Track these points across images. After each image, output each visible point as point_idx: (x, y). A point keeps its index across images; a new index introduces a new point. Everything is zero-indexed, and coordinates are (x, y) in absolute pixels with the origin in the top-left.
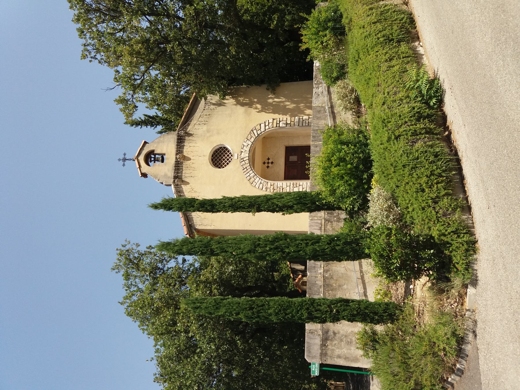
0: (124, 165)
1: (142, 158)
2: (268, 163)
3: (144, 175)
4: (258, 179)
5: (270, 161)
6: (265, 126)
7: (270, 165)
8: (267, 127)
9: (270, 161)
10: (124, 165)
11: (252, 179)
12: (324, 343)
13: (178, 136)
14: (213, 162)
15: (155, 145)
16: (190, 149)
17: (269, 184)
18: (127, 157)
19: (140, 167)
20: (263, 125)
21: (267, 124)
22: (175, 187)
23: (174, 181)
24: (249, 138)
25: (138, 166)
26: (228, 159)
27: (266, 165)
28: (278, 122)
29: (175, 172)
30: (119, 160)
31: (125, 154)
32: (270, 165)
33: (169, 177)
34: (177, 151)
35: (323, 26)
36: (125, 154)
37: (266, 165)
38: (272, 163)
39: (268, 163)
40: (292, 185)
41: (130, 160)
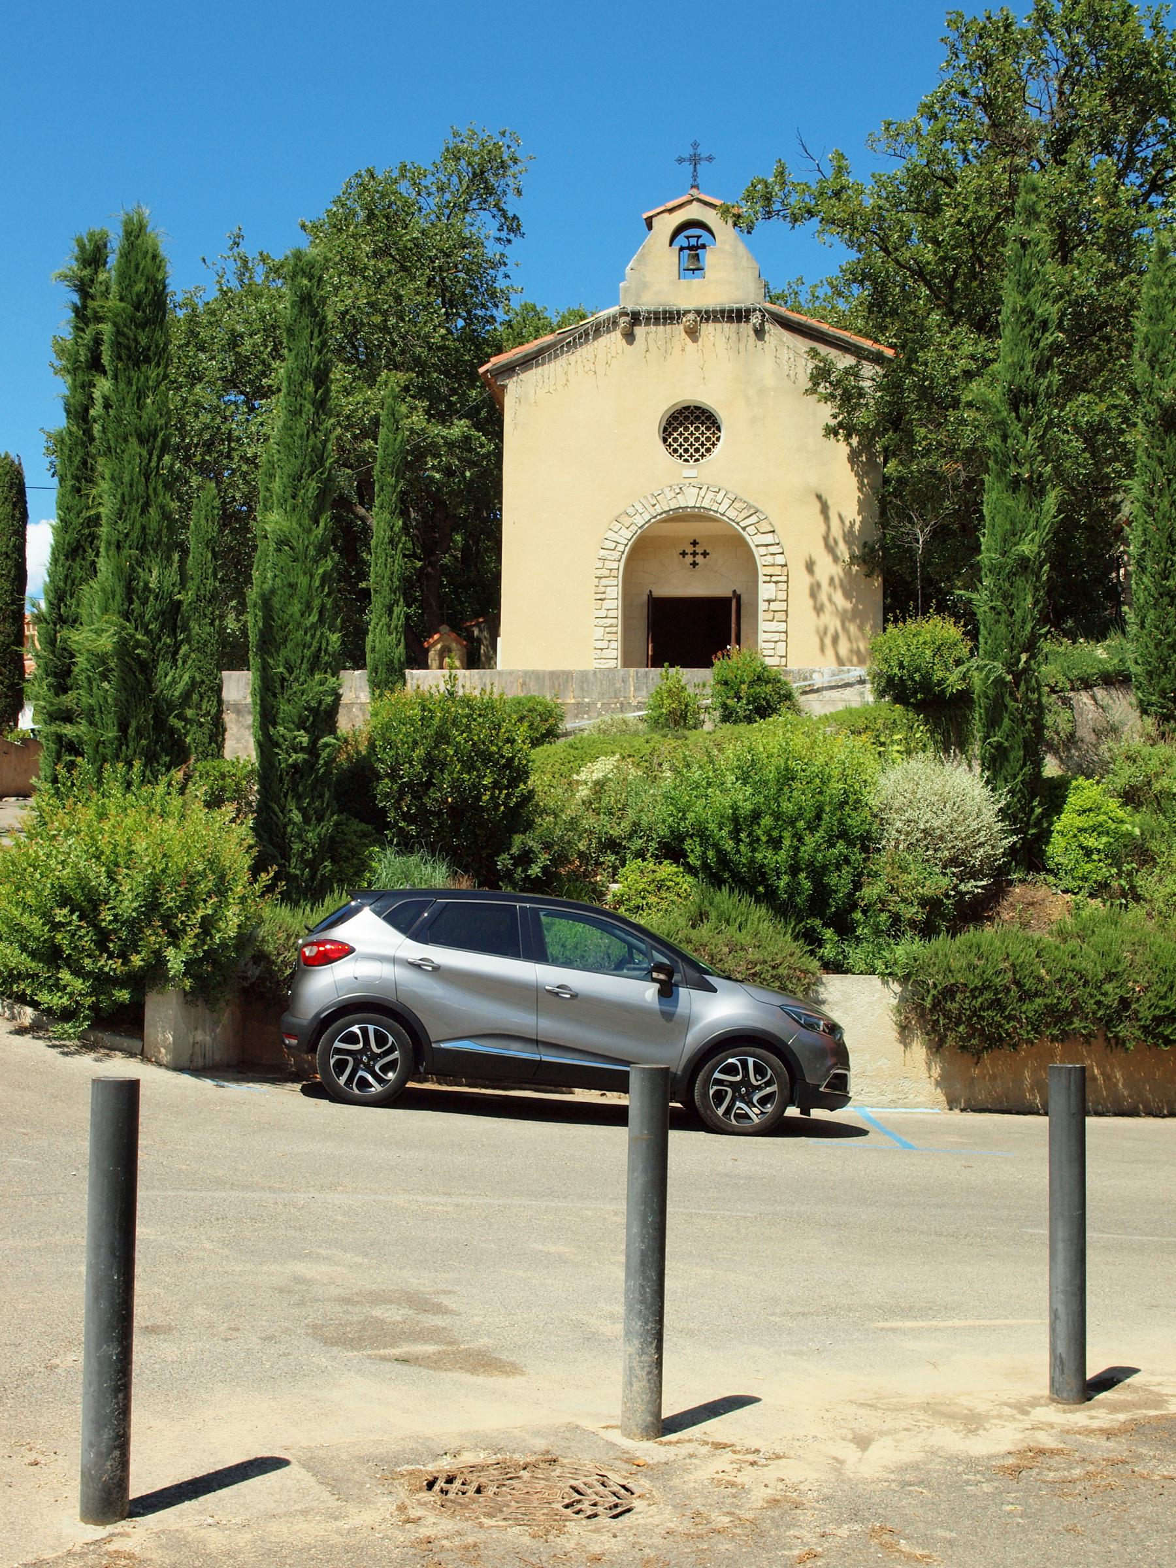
0: (680, 160)
1: (694, 212)
2: (694, 554)
3: (649, 223)
5: (699, 559)
7: (689, 559)
8: (763, 550)
9: (699, 559)
10: (680, 160)
11: (627, 521)
13: (748, 311)
14: (680, 412)
15: (727, 247)
16: (721, 342)
17: (615, 565)
19: (671, 211)
20: (769, 539)
21: (773, 549)
22: (609, 319)
24: (737, 505)
25: (670, 205)
26: (686, 451)
27: (690, 549)
28: (774, 579)
29: (649, 312)
30: (695, 145)
31: (710, 159)
32: (689, 559)
33: (638, 296)
34: (707, 312)
35: (675, 693)
36: (710, 159)
37: (690, 549)
38: (694, 564)
39: (694, 554)
41: (695, 177)
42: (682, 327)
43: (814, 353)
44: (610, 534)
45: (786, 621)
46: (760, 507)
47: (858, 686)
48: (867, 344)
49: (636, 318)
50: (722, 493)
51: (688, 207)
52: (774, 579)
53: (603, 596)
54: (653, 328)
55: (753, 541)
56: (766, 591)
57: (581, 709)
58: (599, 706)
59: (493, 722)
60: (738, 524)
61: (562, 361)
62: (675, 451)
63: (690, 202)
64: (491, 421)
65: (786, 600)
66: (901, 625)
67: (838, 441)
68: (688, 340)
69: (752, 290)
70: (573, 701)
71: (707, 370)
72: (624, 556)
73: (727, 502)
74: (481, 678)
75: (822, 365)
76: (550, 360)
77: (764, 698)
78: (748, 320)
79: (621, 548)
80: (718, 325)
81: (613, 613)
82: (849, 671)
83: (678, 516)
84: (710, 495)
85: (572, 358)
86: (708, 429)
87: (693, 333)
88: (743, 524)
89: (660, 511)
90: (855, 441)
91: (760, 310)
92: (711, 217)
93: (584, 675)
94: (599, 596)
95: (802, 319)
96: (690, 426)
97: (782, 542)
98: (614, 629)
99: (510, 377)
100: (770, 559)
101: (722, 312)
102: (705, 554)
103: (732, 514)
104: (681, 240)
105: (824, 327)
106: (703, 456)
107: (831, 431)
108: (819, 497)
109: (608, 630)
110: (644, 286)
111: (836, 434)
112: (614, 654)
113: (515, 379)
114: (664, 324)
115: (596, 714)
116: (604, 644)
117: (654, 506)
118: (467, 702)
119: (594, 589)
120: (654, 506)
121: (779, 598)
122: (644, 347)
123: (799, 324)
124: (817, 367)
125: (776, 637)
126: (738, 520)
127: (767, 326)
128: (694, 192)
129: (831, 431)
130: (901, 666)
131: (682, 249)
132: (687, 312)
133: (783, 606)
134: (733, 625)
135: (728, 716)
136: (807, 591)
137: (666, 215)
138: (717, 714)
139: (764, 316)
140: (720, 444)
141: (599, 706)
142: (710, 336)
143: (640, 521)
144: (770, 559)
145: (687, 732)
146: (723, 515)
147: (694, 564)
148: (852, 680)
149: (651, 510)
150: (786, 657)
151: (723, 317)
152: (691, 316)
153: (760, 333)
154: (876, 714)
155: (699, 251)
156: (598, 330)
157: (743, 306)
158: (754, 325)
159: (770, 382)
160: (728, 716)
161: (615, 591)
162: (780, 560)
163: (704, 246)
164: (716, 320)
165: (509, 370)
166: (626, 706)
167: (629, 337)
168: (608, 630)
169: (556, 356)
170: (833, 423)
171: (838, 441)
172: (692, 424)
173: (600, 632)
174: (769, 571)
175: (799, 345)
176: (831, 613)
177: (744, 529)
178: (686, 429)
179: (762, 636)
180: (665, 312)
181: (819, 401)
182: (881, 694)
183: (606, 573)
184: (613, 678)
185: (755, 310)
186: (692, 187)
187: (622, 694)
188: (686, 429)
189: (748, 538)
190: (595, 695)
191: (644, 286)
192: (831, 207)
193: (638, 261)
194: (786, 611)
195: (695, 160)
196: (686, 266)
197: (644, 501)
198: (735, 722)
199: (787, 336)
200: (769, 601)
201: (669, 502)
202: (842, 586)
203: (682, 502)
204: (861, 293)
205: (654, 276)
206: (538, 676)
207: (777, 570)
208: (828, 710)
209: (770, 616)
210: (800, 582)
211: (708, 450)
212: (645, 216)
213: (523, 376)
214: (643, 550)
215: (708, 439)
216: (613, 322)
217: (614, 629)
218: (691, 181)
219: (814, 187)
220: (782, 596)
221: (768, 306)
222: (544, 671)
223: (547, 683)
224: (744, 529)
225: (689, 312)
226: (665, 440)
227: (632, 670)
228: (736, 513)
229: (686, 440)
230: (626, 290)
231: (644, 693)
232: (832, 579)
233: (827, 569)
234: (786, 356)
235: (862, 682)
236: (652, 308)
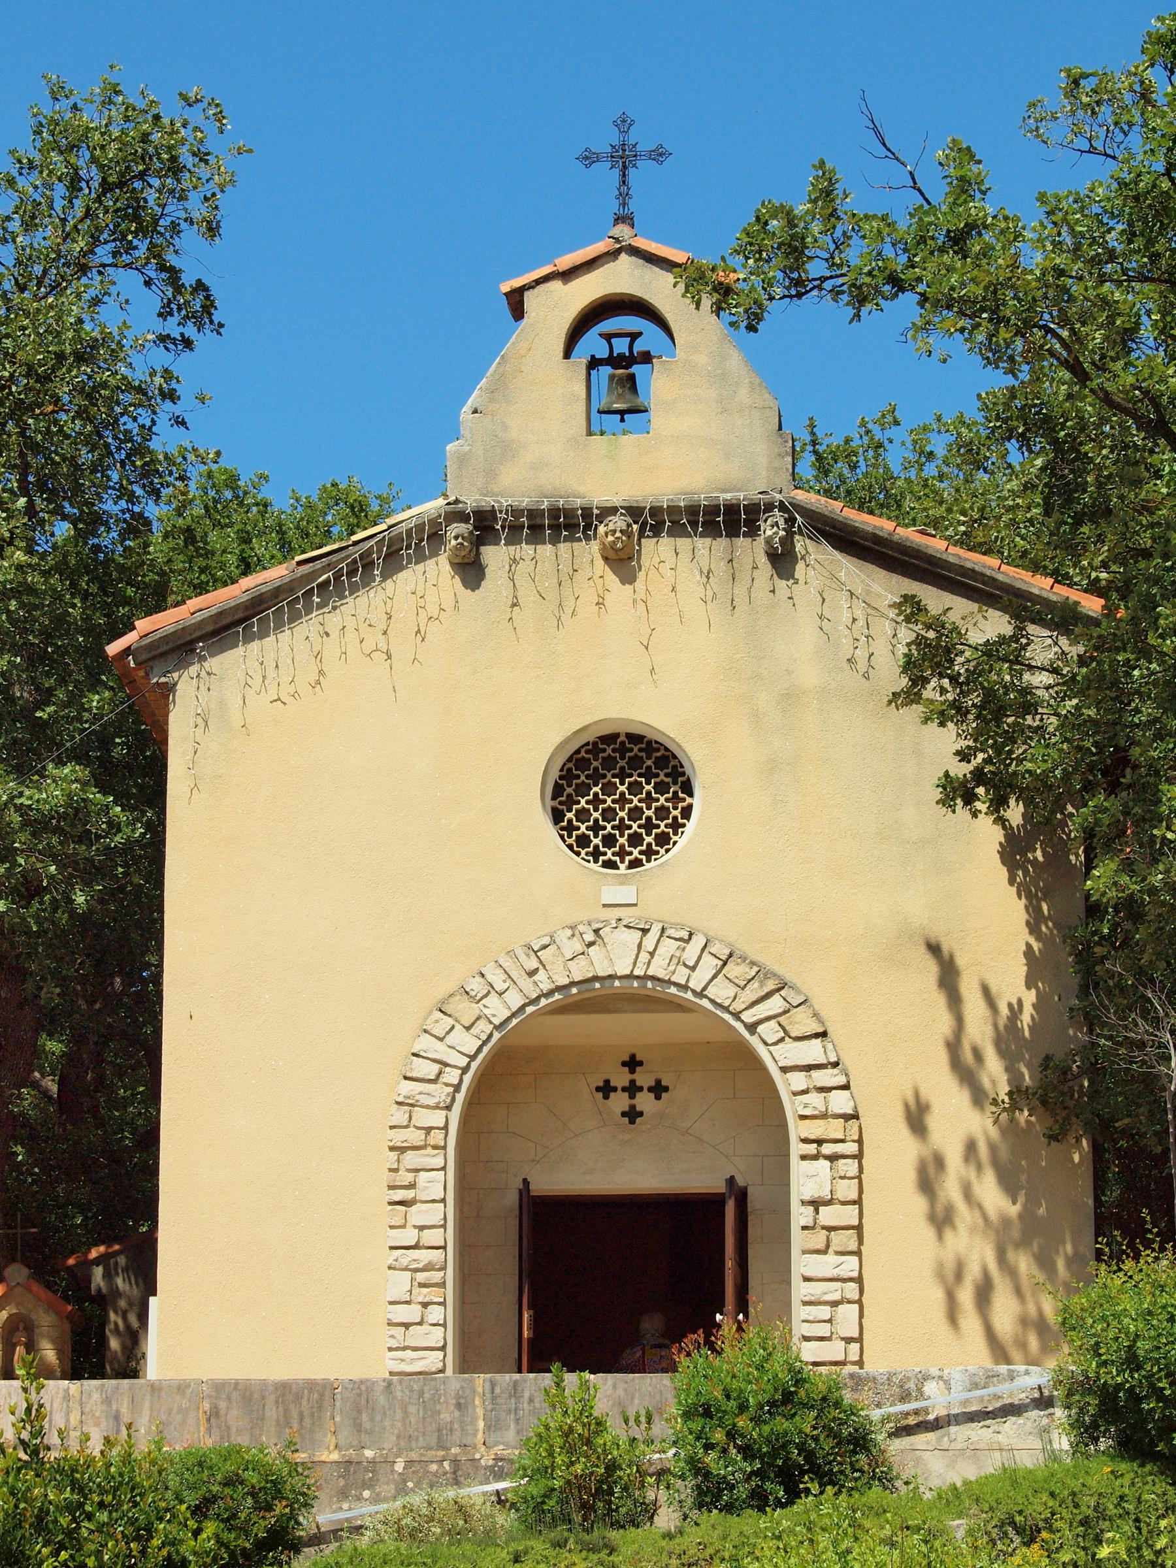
0: (589, 159)
1: (622, 278)
2: (632, 1089)
3: (516, 303)
4: (471, 1046)
5: (645, 1101)
6: (809, 1068)
7: (620, 1102)
8: (798, 1080)
9: (645, 1101)
10: (589, 159)
11: (465, 1010)
17: (437, 1118)
18: (641, 174)
19: (567, 275)
20: (813, 1052)
22: (420, 527)
23: (462, 517)
25: (565, 261)
26: (609, 841)
27: (621, 1078)
28: (827, 1149)
29: (516, 512)
30: (624, 124)
31: (659, 155)
32: (620, 1102)
33: (491, 474)
34: (655, 511)
35: (583, 1435)
36: (659, 155)
37: (621, 1078)
38: (632, 1115)
39: (632, 1089)
40: (425, 1256)
41: (624, 198)
42: (595, 546)
43: (912, 609)
44: (425, 1044)
45: (858, 1253)
46: (789, 976)
47: (1034, 1414)
48: (1040, 584)
49: (485, 526)
50: (698, 942)
51: (609, 268)
52: (827, 1149)
53: (408, 1194)
54: (527, 550)
55: (776, 1055)
56: (808, 1179)
57: (355, 1476)
58: (399, 1467)
59: (133, 1522)
60: (737, 1016)
61: (308, 627)
63: (613, 255)
64: (136, 768)
65: (858, 1202)
66: (1129, 1265)
67: (975, 814)
68: (611, 579)
69: (763, 461)
70: (335, 1456)
71: (661, 648)
72: (460, 1097)
73: (709, 965)
74: (107, 1401)
75: (931, 635)
76: (279, 626)
77: (804, 1450)
78: (753, 531)
79: (452, 1076)
80: (683, 543)
81: (434, 1237)
82: (1011, 1377)
83: (592, 998)
84: (669, 947)
85: (333, 620)
86: (661, 788)
87: (622, 562)
88: (748, 1017)
89: (546, 986)
90: (1015, 813)
91: (782, 507)
92: (660, 290)
93: (361, 1391)
94: (400, 1195)
95: (881, 525)
96: (618, 786)
97: (846, 1060)
98: (437, 1276)
99: (183, 665)
100: (815, 1101)
101: (693, 510)
102: (658, 1089)
103: (721, 991)
104: (592, 344)
105: (936, 545)
106: (649, 853)
107: (956, 792)
108: (934, 949)
109: (421, 1277)
110: (505, 450)
111: (969, 798)
112: (436, 1336)
113: (194, 669)
114: (555, 541)
115: (386, 1489)
116: (410, 1313)
117: (532, 973)
118: (70, 1474)
119: (386, 1178)
120: (532, 973)
121: (839, 1195)
122: (506, 594)
123: (876, 539)
124: (919, 641)
125: (834, 1291)
126: (737, 1006)
127: (800, 544)
128: (623, 231)
129: (956, 792)
130: (1132, 1361)
131: (594, 363)
132: (608, 511)
133: (849, 1215)
134: (729, 1264)
135: (711, 1494)
136: (910, 1177)
137: (556, 285)
138: (686, 1489)
139: (790, 521)
140: (691, 826)
141: (399, 1467)
142: (665, 569)
143: (498, 1010)
144: (815, 1101)
145: (614, 1535)
146: (700, 994)
147: (632, 1115)
148: (1020, 1397)
149: (525, 983)
150: (860, 1340)
151: (694, 524)
152: (618, 522)
153: (782, 560)
154: (1075, 1485)
155: (635, 369)
156: (395, 554)
157: (740, 496)
158: (769, 541)
159: (810, 675)
160: (711, 1494)
161: (437, 1184)
162: (840, 1102)
163: (646, 358)
164: (677, 530)
165: (183, 648)
166: (466, 1467)
167: (470, 571)
168: (421, 1277)
169: (295, 617)
170: (960, 770)
171: (975, 814)
172: (622, 776)
173: (400, 1284)
174: (815, 1129)
175: (876, 588)
176: (972, 1230)
177: (752, 1028)
178: (609, 789)
179: (800, 1290)
180: (555, 512)
181: (926, 720)
182: (1086, 1432)
183: (417, 1137)
184: (436, 1399)
185: (769, 507)
186: (619, 220)
187: (456, 1436)
188: (609, 789)
189: (762, 1051)
190: (389, 1442)
191: (505, 450)
192: (945, 265)
193: (491, 391)
194: (859, 1228)
195: (624, 158)
196: (604, 404)
197: (507, 963)
198: (729, 1508)
199: (847, 567)
200: (816, 1204)
201: (565, 967)
202: (996, 1164)
203: (599, 963)
204: (1024, 462)
205: (529, 427)
206: (248, 1395)
207: (834, 1129)
208: (965, 1472)
209: (818, 1239)
210: (893, 1155)
211: (663, 840)
212: (505, 287)
213: (214, 663)
214: (506, 1080)
215: (662, 813)
216: (428, 537)
217: (437, 1276)
218: (614, 207)
219: (904, 224)
220: (848, 1190)
221: (801, 496)
222: (264, 1382)
223: (272, 1412)
224: (752, 1028)
225: (613, 510)
226: (557, 816)
227: (481, 1380)
228: (731, 991)
229: (609, 814)
230: (463, 460)
231: (510, 1435)
232: (970, 1148)
233: (959, 1121)
234: (844, 615)
235: (1043, 1402)
236: (525, 503)
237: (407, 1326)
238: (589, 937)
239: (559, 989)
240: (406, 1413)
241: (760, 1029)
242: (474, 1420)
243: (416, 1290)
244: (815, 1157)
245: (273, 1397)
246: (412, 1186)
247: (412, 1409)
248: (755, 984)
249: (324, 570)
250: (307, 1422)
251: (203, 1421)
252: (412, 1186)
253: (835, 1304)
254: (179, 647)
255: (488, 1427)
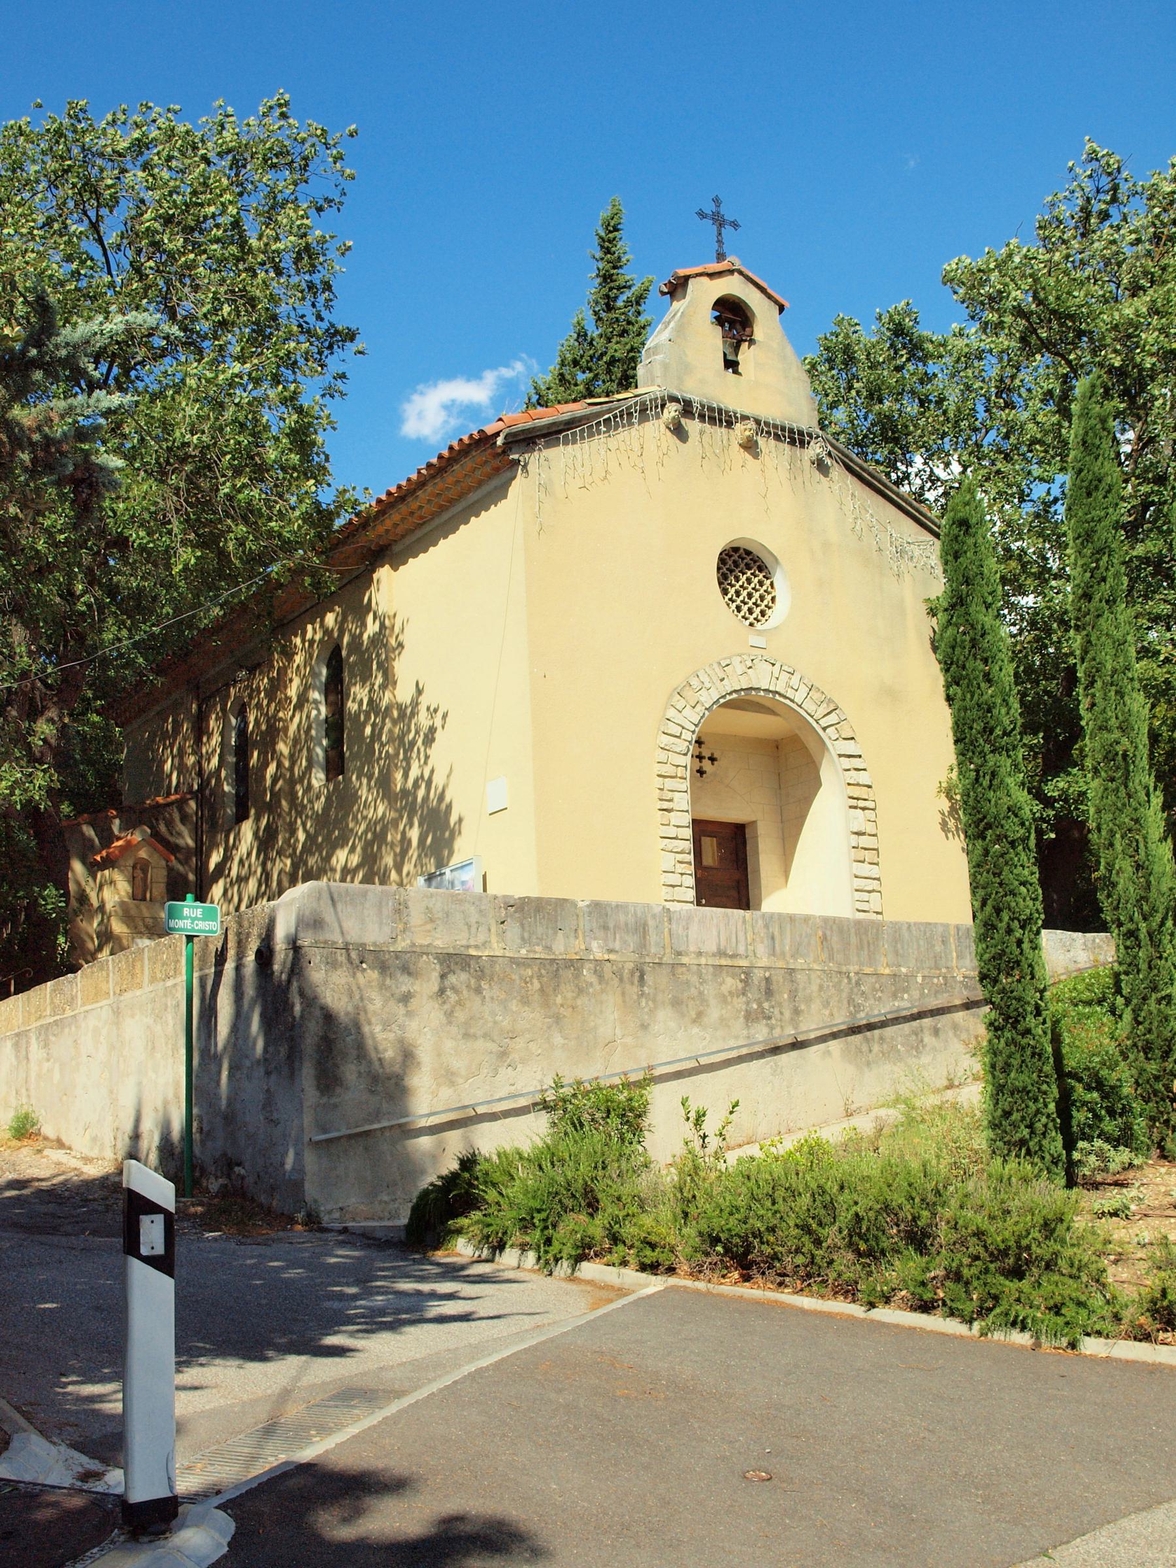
12: (370, 958)
18: (727, 231)
19: (711, 276)
28: (861, 804)
34: (767, 424)
49: (687, 409)
62: (739, 609)
85: (613, 443)
94: (666, 805)
103: (809, 706)
117: (722, 680)
121: (868, 831)
132: (745, 418)
137: (705, 279)
177: (824, 729)
190: (912, 963)
199: (850, 479)
213: (548, 453)
224: (824, 729)
228: (814, 707)
237: (673, 886)
238: (749, 664)
239: (735, 691)
240: (919, 946)
241: (828, 730)
242: (951, 953)
243: (678, 865)
244: (856, 808)
245: (853, 931)
246: (671, 800)
247: (921, 943)
248: (824, 705)
249: (609, 411)
250: (872, 947)
251: (819, 943)
252: (671, 800)
253: (869, 892)
254: (524, 440)
255: (958, 957)
